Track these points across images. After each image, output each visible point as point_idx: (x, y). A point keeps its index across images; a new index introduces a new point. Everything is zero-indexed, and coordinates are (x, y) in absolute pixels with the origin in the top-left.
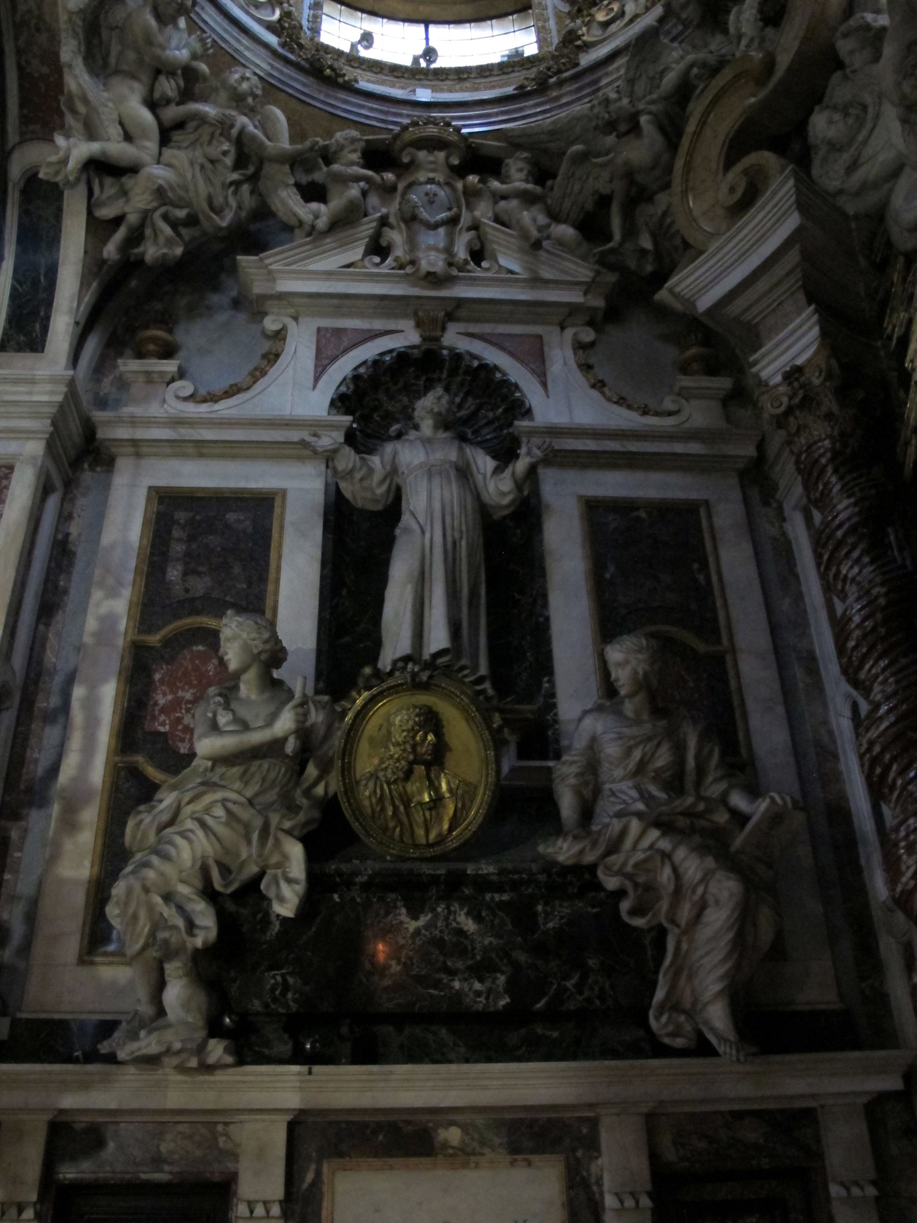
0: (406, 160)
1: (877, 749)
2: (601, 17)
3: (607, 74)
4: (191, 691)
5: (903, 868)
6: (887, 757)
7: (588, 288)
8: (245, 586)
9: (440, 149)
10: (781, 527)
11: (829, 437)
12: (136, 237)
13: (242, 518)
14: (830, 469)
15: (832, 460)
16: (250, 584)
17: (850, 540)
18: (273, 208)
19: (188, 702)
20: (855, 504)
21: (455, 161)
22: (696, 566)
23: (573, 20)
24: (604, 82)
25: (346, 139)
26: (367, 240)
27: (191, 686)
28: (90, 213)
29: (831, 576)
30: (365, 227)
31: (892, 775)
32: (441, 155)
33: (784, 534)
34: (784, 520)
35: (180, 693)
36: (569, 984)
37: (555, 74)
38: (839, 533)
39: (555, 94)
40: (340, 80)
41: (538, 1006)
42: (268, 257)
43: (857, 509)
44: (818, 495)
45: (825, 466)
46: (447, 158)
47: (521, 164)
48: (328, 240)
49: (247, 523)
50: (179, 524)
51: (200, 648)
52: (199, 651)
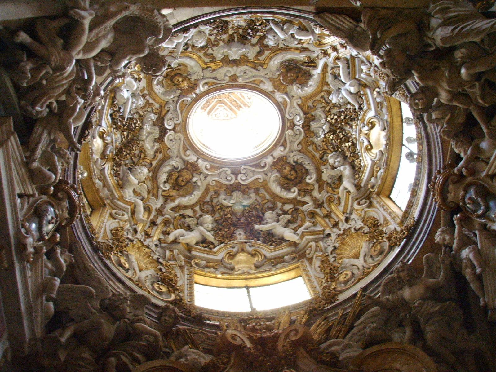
0: (60, 195)
2: (123, 260)
3: (114, 283)
7: (33, 338)
9: (69, 214)
12: (31, 54)
18: (35, 129)
21: (63, 224)
23: (113, 244)
24: (111, 282)
25: (68, 159)
26: (23, 192)
28: (38, 18)
30: (30, 188)
32: (66, 215)
37: (102, 253)
39: (96, 258)
40: (82, 140)
42: (15, 138)
46: (66, 219)
47: (68, 260)
48: (23, 170)
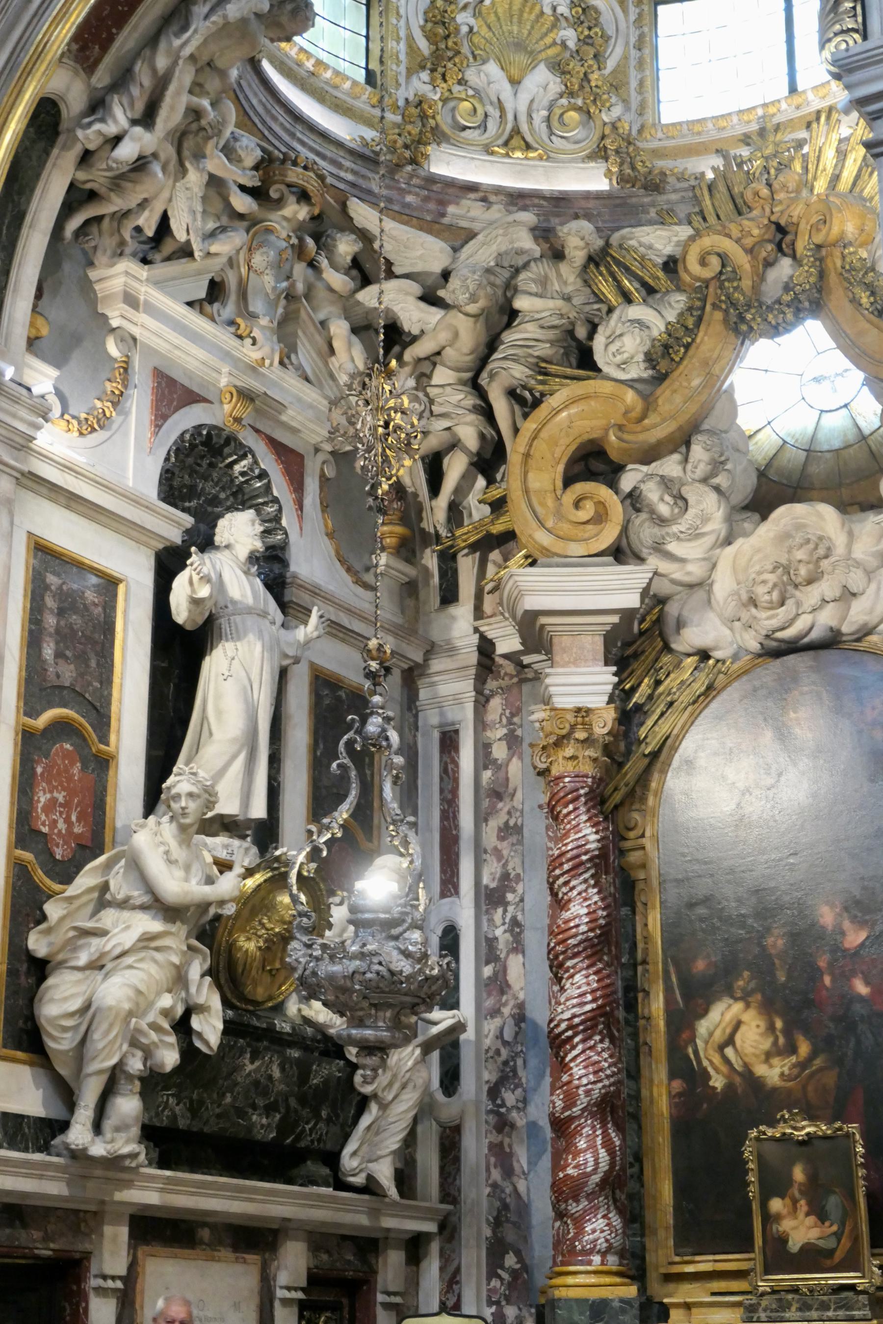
1: (577, 1020)
4: (63, 793)
5: (579, 1102)
6: (581, 1028)
8: (98, 685)
10: (415, 736)
11: (593, 778)
13: (96, 600)
14: (583, 799)
15: (586, 794)
16: (101, 683)
17: (588, 865)
19: (61, 805)
20: (598, 841)
22: (367, 760)
27: (64, 789)
29: (561, 880)
31: (577, 1040)
33: (415, 743)
34: (417, 729)
35: (56, 794)
36: (308, 1127)
38: (584, 858)
41: (288, 1141)
43: (600, 845)
44: (565, 811)
45: (580, 796)
49: (100, 609)
50: (51, 591)
51: (68, 746)
52: (67, 750)
